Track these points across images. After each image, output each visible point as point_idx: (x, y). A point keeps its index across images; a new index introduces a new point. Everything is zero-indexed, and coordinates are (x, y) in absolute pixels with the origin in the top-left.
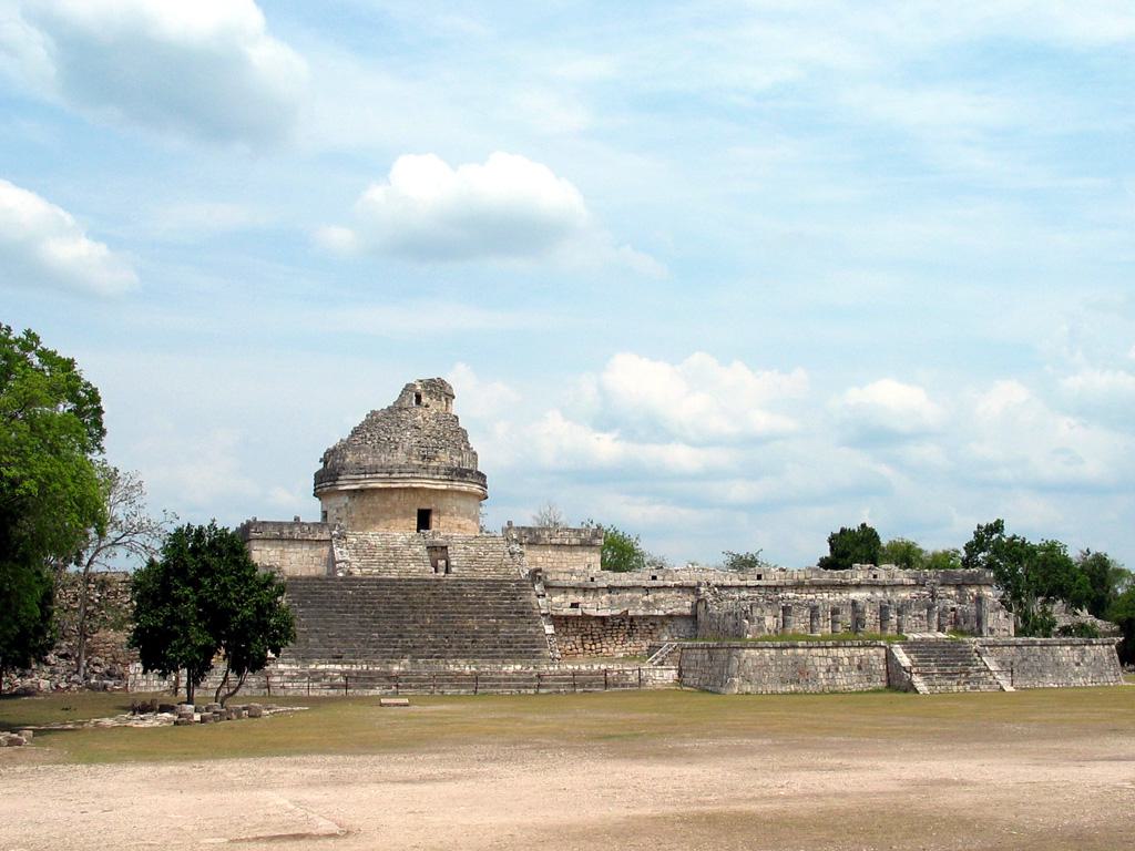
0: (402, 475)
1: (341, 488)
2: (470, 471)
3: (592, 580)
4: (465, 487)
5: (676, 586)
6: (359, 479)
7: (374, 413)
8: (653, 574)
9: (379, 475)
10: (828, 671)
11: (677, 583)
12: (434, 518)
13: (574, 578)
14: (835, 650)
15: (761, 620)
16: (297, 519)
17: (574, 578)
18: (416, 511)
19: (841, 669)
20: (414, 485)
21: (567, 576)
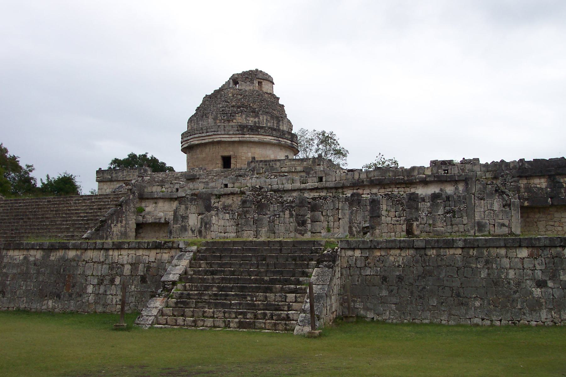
0: (208, 134)
2: (262, 128)
3: (177, 190)
4: (256, 138)
6: (188, 140)
8: (225, 182)
10: (100, 283)
11: (242, 189)
12: (232, 161)
13: (164, 189)
14: (116, 253)
15: (185, 218)
18: (220, 157)
19: (118, 281)
20: (215, 140)
21: (159, 189)
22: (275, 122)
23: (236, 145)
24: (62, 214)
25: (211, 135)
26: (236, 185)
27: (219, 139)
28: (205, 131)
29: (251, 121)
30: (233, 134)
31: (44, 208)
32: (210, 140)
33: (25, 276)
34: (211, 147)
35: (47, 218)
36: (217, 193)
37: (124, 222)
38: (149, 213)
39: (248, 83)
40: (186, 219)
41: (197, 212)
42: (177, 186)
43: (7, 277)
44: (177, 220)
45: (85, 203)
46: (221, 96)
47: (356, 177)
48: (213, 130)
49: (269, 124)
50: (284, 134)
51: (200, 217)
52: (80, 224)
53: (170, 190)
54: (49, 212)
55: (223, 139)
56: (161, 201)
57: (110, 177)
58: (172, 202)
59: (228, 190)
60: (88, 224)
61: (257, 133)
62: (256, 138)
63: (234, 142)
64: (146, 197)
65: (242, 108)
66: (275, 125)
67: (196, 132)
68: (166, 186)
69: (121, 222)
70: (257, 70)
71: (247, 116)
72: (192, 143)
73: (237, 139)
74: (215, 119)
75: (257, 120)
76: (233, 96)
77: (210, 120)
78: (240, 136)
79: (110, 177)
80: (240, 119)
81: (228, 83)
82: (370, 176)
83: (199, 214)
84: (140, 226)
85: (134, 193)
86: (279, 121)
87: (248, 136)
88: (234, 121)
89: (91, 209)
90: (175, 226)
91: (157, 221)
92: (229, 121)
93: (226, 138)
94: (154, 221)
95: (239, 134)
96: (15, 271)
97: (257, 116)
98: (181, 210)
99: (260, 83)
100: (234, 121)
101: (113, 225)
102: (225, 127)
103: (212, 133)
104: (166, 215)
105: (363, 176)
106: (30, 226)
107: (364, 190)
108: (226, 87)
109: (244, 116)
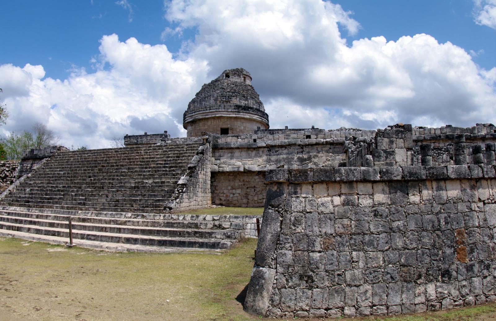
0: (211, 111)
1: (186, 121)
2: (252, 108)
3: (255, 141)
4: (247, 116)
5: (327, 143)
6: (193, 116)
7: (205, 85)
9: (200, 112)
11: (328, 140)
12: (230, 132)
13: (240, 140)
15: (390, 153)
16: (146, 133)
17: (240, 140)
18: (220, 129)
20: (217, 115)
21: (234, 139)
22: (258, 105)
23: (233, 120)
24: (137, 162)
25: (214, 112)
26: (319, 136)
27: (220, 115)
28: (209, 109)
29: (243, 103)
30: (231, 112)
31: (114, 157)
32: (213, 116)
33: (359, 239)
34: (213, 121)
35: (122, 166)
36: (302, 143)
37: (205, 170)
38: (224, 163)
39: (237, 77)
40: (391, 154)
41: (406, 146)
42: (253, 138)
43: (311, 243)
44: (379, 156)
45: (157, 152)
46: (218, 85)
47: (433, 132)
48: (216, 108)
49: (254, 107)
50: (264, 115)
51: (409, 153)
52: (163, 171)
53: (246, 141)
54: (121, 160)
55: (223, 115)
56: (237, 150)
57: (136, 141)
58: (250, 152)
59: (313, 140)
60: (174, 170)
61: (248, 112)
62: (247, 116)
63: (231, 118)
64: (221, 146)
65: (235, 93)
66: (258, 108)
67: (200, 110)
68: (242, 137)
69: (203, 170)
70: (242, 69)
71: (240, 99)
72: (196, 118)
73: (234, 116)
74: (216, 100)
75: (246, 102)
76: (228, 84)
77: (212, 101)
78: (237, 113)
79: (136, 141)
80: (236, 101)
81: (222, 75)
82: (443, 132)
83: (409, 149)
84: (214, 174)
85: (209, 143)
86: (260, 105)
87: (242, 114)
88: (231, 102)
89: (168, 157)
90: (376, 163)
91: (236, 169)
92: (227, 102)
93: (225, 115)
94: (231, 170)
95: (236, 112)
96: (328, 229)
97: (247, 100)
98: (384, 144)
99: (244, 78)
100: (231, 102)
101: (199, 172)
102: (224, 106)
103: (215, 110)
104: (244, 164)
105: (438, 132)
106: (107, 173)
107: (439, 143)
108: (221, 78)
109: (238, 99)
